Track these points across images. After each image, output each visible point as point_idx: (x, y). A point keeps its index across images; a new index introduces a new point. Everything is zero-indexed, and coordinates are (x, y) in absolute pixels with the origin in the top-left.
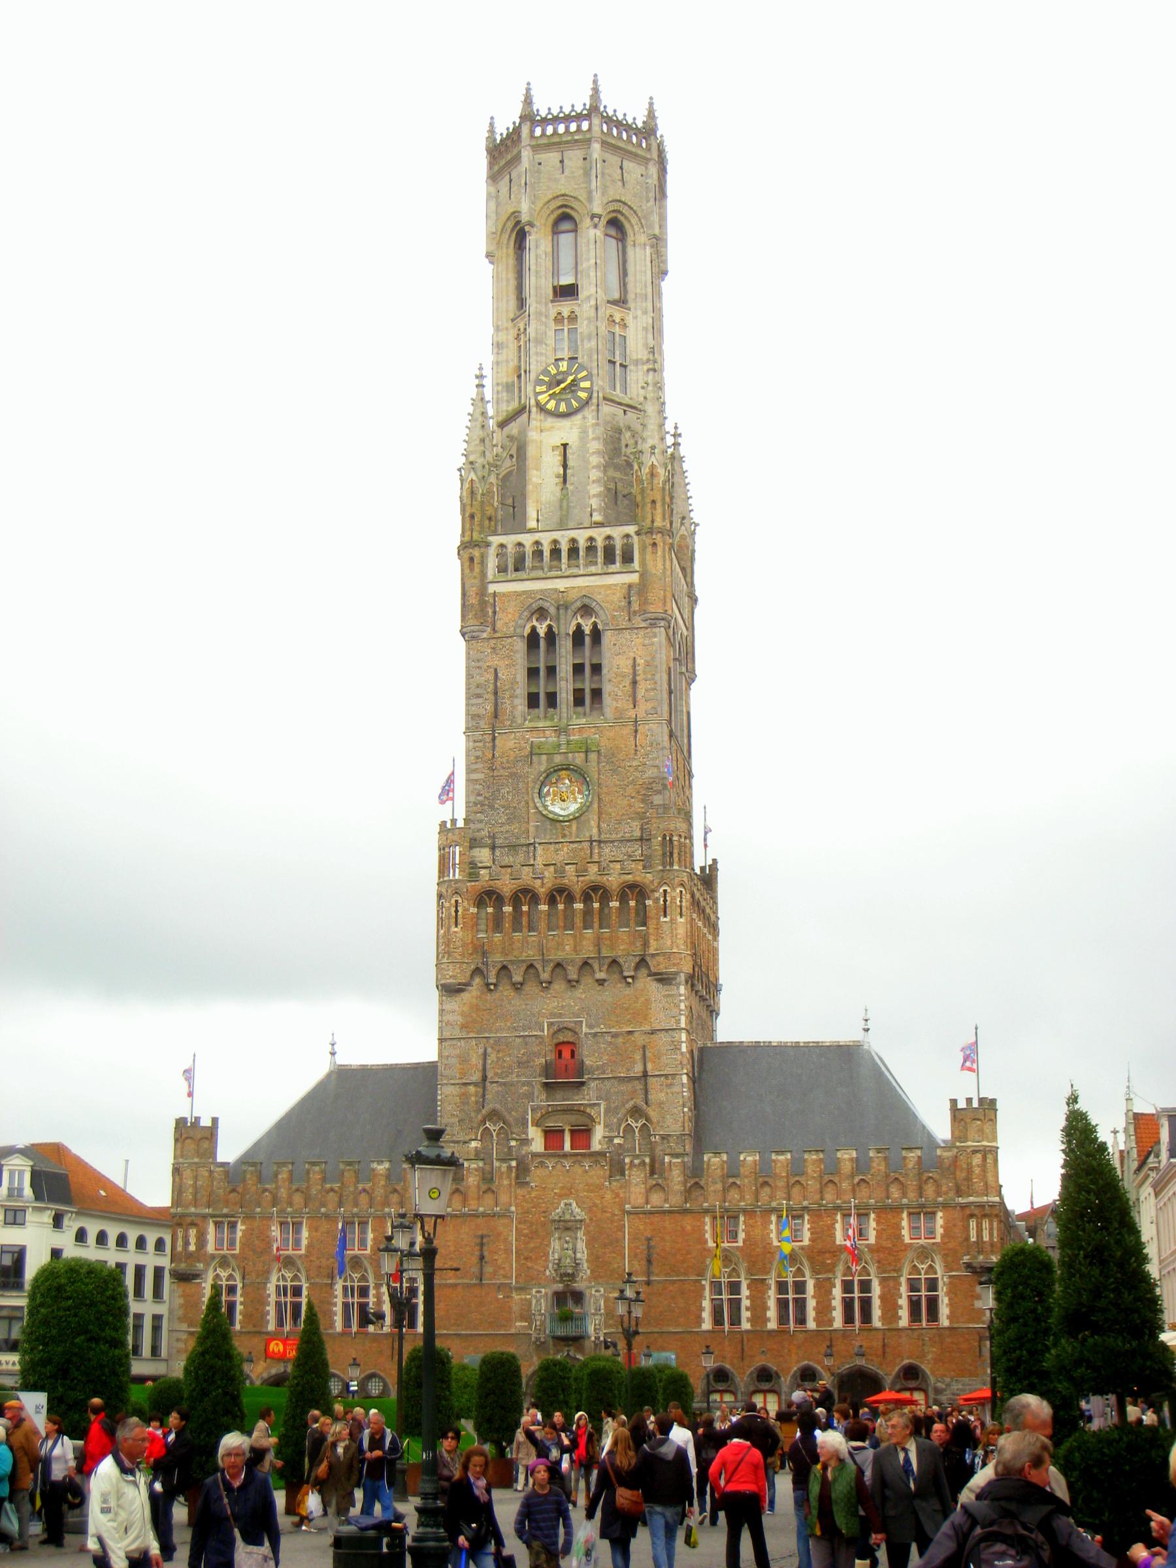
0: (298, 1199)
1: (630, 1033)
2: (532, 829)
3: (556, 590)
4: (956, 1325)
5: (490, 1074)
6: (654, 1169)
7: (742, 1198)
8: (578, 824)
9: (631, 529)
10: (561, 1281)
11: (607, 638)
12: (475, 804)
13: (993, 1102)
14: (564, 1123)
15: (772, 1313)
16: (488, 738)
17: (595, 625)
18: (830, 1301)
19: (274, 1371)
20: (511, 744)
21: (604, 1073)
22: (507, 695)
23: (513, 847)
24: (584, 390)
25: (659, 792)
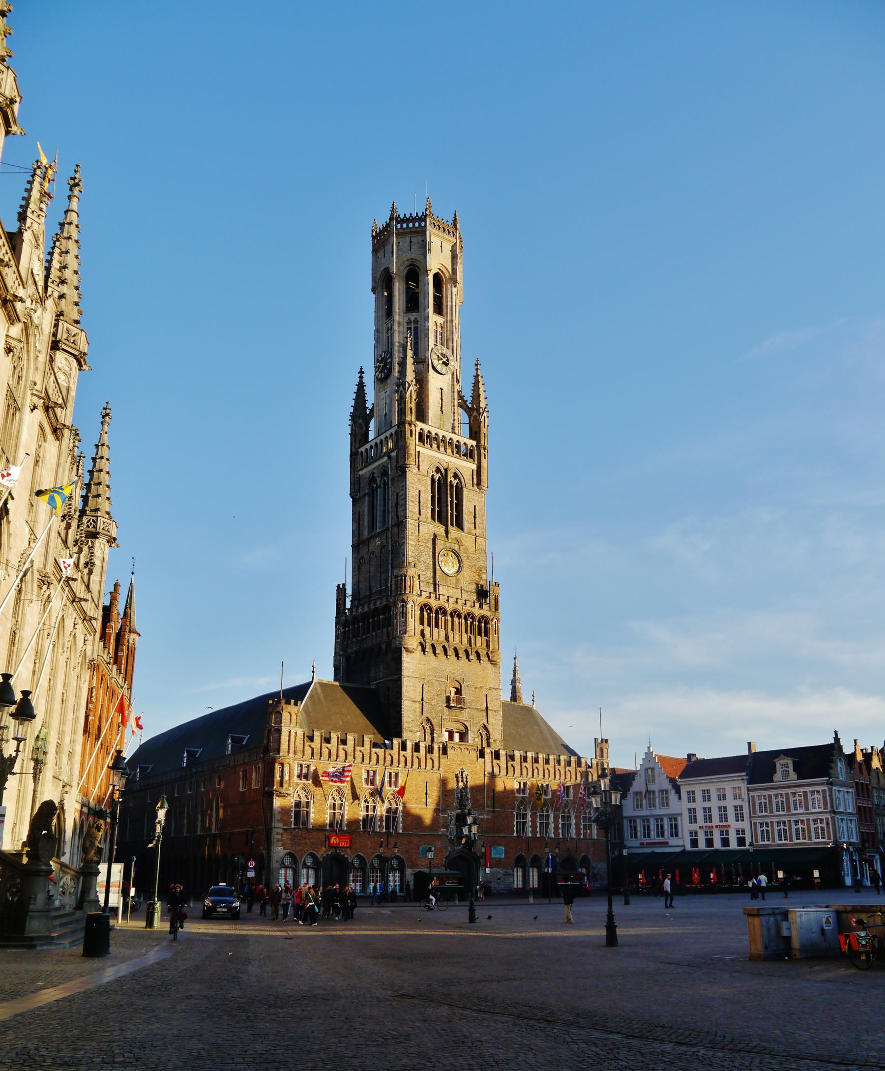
0: (342, 754)
1: (481, 687)
2: (437, 577)
3: (444, 460)
4: (600, 838)
5: (425, 698)
6: (497, 755)
7: (527, 774)
8: (456, 579)
9: (474, 443)
10: (459, 809)
11: (465, 491)
12: (412, 557)
13: (606, 741)
14: (456, 727)
15: (538, 830)
16: (417, 525)
17: (457, 483)
18: (558, 824)
19: (330, 853)
20: (426, 531)
21: (471, 705)
22: (425, 505)
23: (428, 584)
24: (452, 365)
25: (484, 573)
